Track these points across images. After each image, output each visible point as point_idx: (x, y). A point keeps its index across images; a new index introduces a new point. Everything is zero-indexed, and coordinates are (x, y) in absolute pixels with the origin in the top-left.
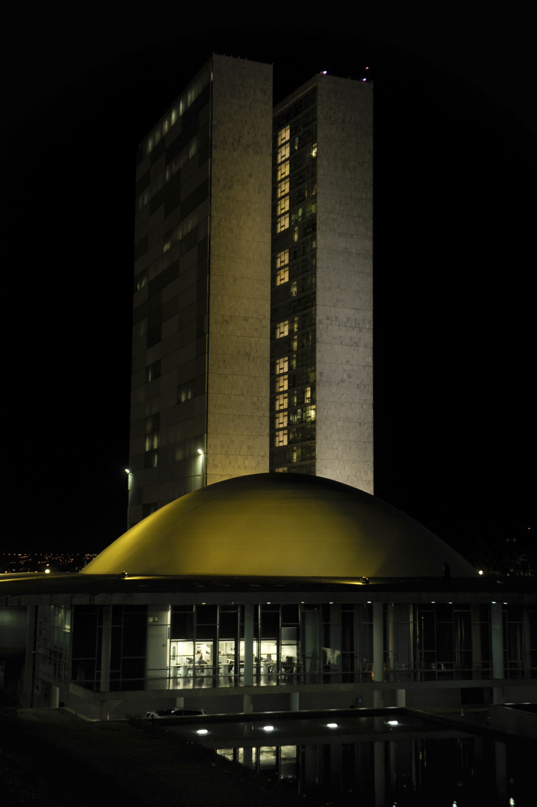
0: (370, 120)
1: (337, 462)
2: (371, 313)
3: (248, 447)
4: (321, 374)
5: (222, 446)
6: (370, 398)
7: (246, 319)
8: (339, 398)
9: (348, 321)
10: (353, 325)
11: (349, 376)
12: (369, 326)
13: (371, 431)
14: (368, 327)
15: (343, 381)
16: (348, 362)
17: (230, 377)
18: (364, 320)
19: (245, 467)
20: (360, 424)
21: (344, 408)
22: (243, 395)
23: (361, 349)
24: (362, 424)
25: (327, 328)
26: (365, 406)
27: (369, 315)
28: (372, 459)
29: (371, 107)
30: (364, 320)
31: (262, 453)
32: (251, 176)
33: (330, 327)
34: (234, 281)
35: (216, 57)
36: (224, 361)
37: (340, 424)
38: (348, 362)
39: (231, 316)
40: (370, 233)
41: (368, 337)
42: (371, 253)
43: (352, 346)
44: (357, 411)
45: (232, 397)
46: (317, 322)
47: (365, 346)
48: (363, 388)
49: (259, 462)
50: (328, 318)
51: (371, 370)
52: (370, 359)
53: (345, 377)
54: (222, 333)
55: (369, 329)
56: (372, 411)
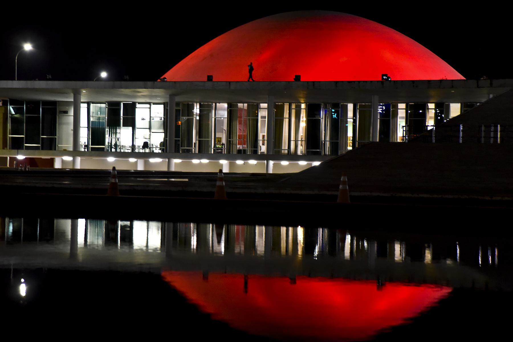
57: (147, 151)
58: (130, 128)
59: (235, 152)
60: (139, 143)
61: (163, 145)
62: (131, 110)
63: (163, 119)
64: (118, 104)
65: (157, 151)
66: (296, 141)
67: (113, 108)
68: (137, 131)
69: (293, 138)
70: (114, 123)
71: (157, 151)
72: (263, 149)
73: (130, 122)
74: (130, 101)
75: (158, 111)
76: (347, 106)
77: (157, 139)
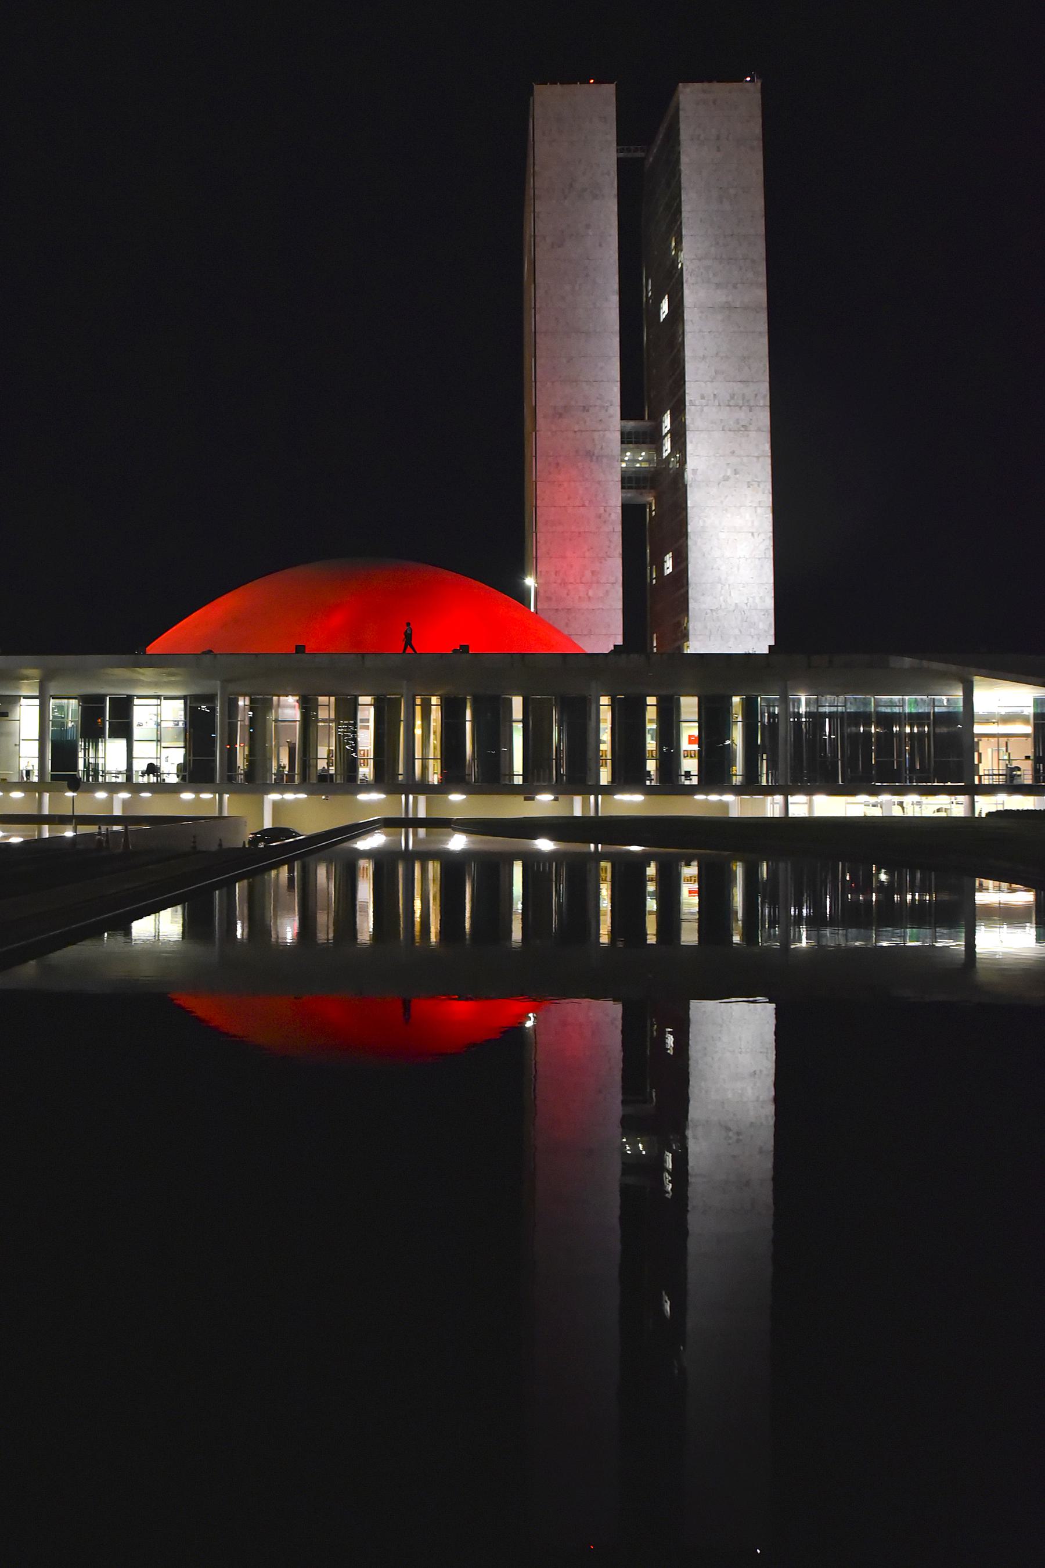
0: (758, 130)
1: (720, 586)
2: (767, 385)
3: (593, 572)
4: (694, 471)
5: (556, 573)
6: (767, 499)
8: (722, 502)
9: (732, 397)
10: (741, 403)
11: (736, 472)
12: (765, 401)
13: (769, 543)
14: (761, 403)
15: (726, 479)
16: (733, 452)
17: (566, 485)
18: (756, 395)
19: (589, 598)
20: (753, 534)
21: (729, 515)
22: (584, 506)
23: (753, 434)
24: (756, 535)
25: (702, 410)
26: (759, 510)
27: (764, 387)
29: (758, 113)
30: (756, 395)
31: (612, 579)
33: (705, 409)
34: (568, 362)
36: (558, 464)
38: (733, 452)
39: (565, 407)
40: (763, 279)
41: (764, 418)
42: (765, 305)
43: (739, 430)
44: (748, 516)
45: (570, 510)
46: (687, 404)
47: (759, 430)
48: (756, 484)
49: (607, 592)
50: (703, 397)
51: (769, 461)
52: (767, 447)
53: (729, 473)
54: (554, 428)
55: (764, 406)
56: (770, 516)
57: (153, 779)
58: (122, 743)
59: (314, 780)
60: (139, 766)
61: (182, 769)
62: (123, 708)
63: (181, 724)
64: (101, 698)
65: (173, 779)
66: (425, 759)
67: (91, 707)
68: (136, 745)
69: (418, 754)
70: (92, 733)
71: (173, 779)
72: (366, 771)
73: (124, 729)
74: (123, 692)
75: (174, 711)
76: (511, 700)
77: (172, 759)
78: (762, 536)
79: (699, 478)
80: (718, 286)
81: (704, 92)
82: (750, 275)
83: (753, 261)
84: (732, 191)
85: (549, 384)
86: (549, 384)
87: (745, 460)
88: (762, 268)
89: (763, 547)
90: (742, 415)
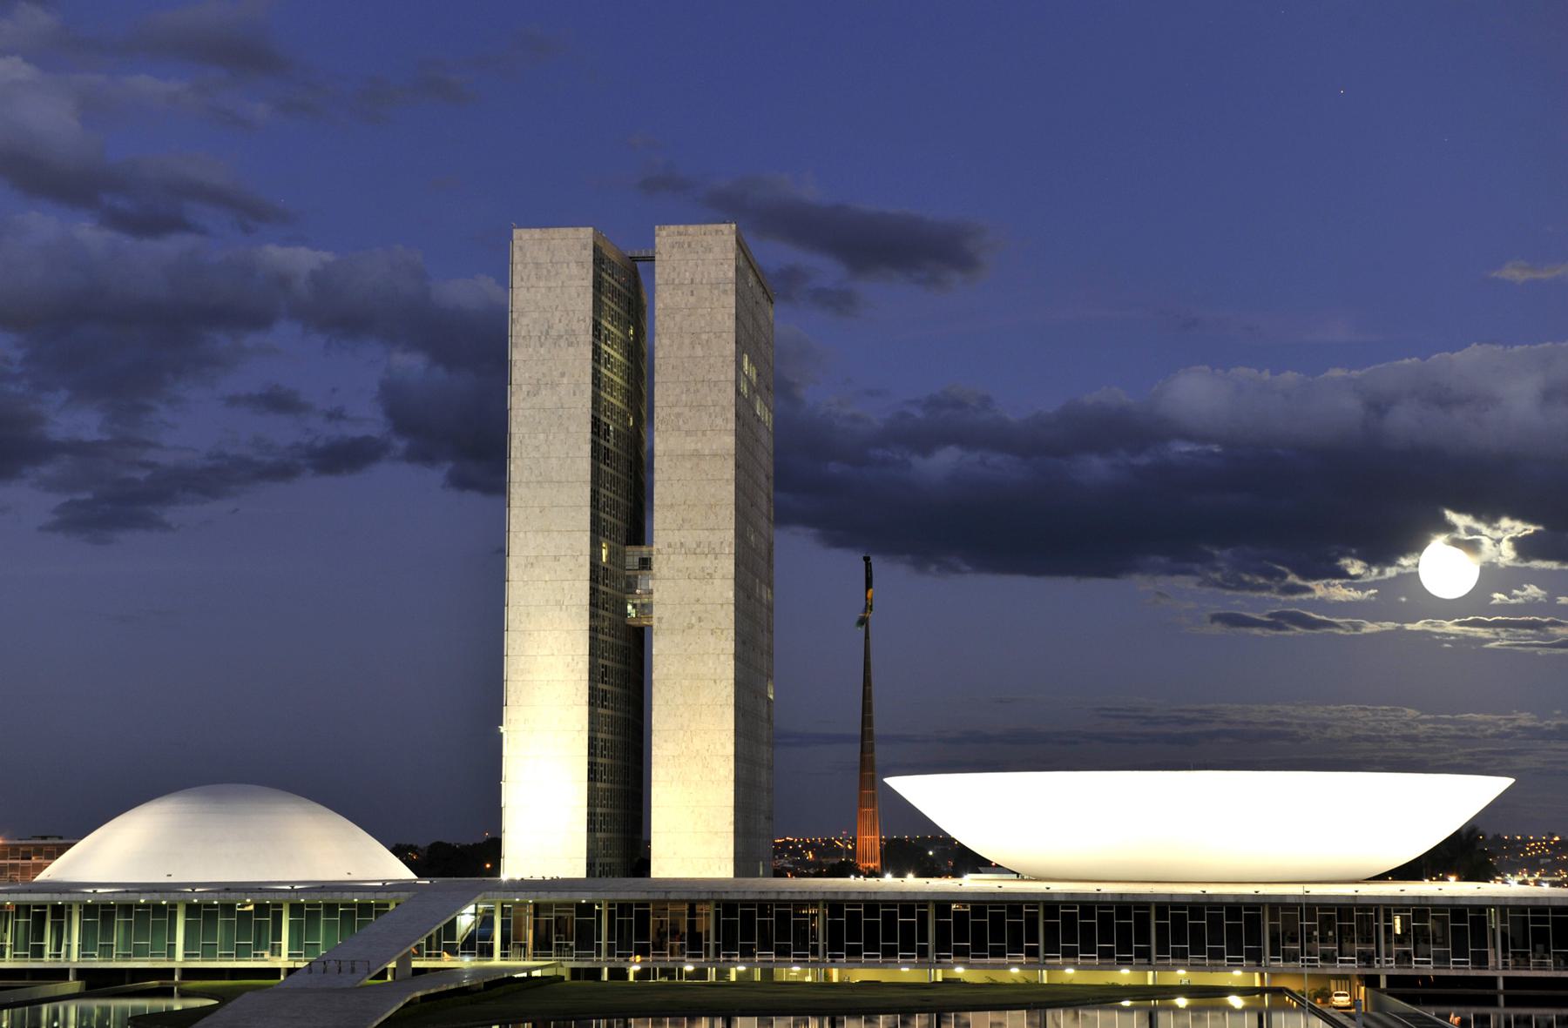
4: (660, 619)
7: (556, 558)
11: (700, 620)
12: (729, 549)
15: (691, 626)
27: (730, 535)
28: (733, 727)
29: (733, 256)
32: (563, 375)
35: (516, 233)
37: (686, 683)
40: (732, 426)
41: (728, 565)
47: (724, 577)
51: (732, 608)
52: (731, 594)
53: (694, 620)
56: (732, 663)
78: (724, 683)
79: (664, 626)
80: (688, 433)
81: (680, 234)
82: (719, 421)
83: (723, 408)
84: (704, 337)
85: (522, 535)
86: (522, 535)
87: (709, 607)
88: (731, 415)
89: (724, 694)
90: (708, 563)
